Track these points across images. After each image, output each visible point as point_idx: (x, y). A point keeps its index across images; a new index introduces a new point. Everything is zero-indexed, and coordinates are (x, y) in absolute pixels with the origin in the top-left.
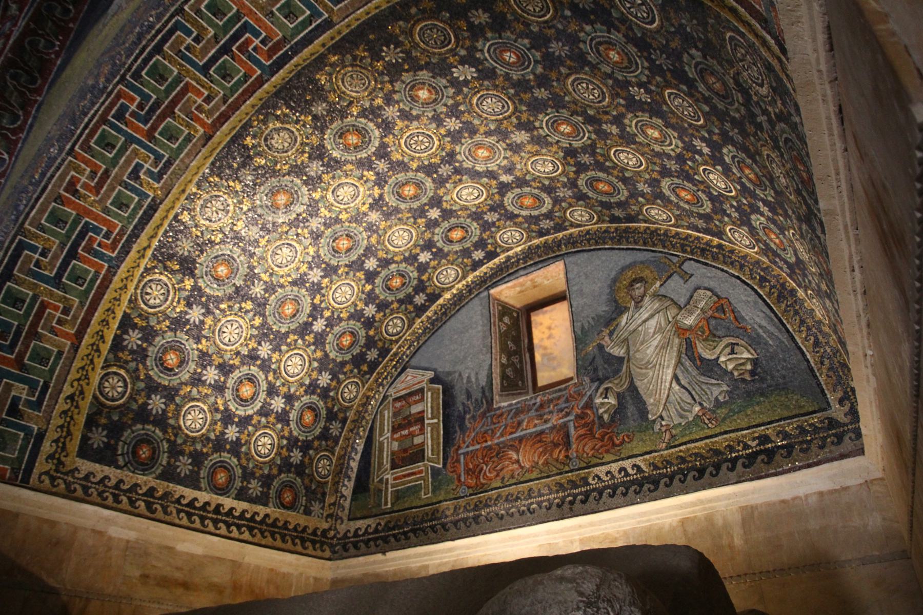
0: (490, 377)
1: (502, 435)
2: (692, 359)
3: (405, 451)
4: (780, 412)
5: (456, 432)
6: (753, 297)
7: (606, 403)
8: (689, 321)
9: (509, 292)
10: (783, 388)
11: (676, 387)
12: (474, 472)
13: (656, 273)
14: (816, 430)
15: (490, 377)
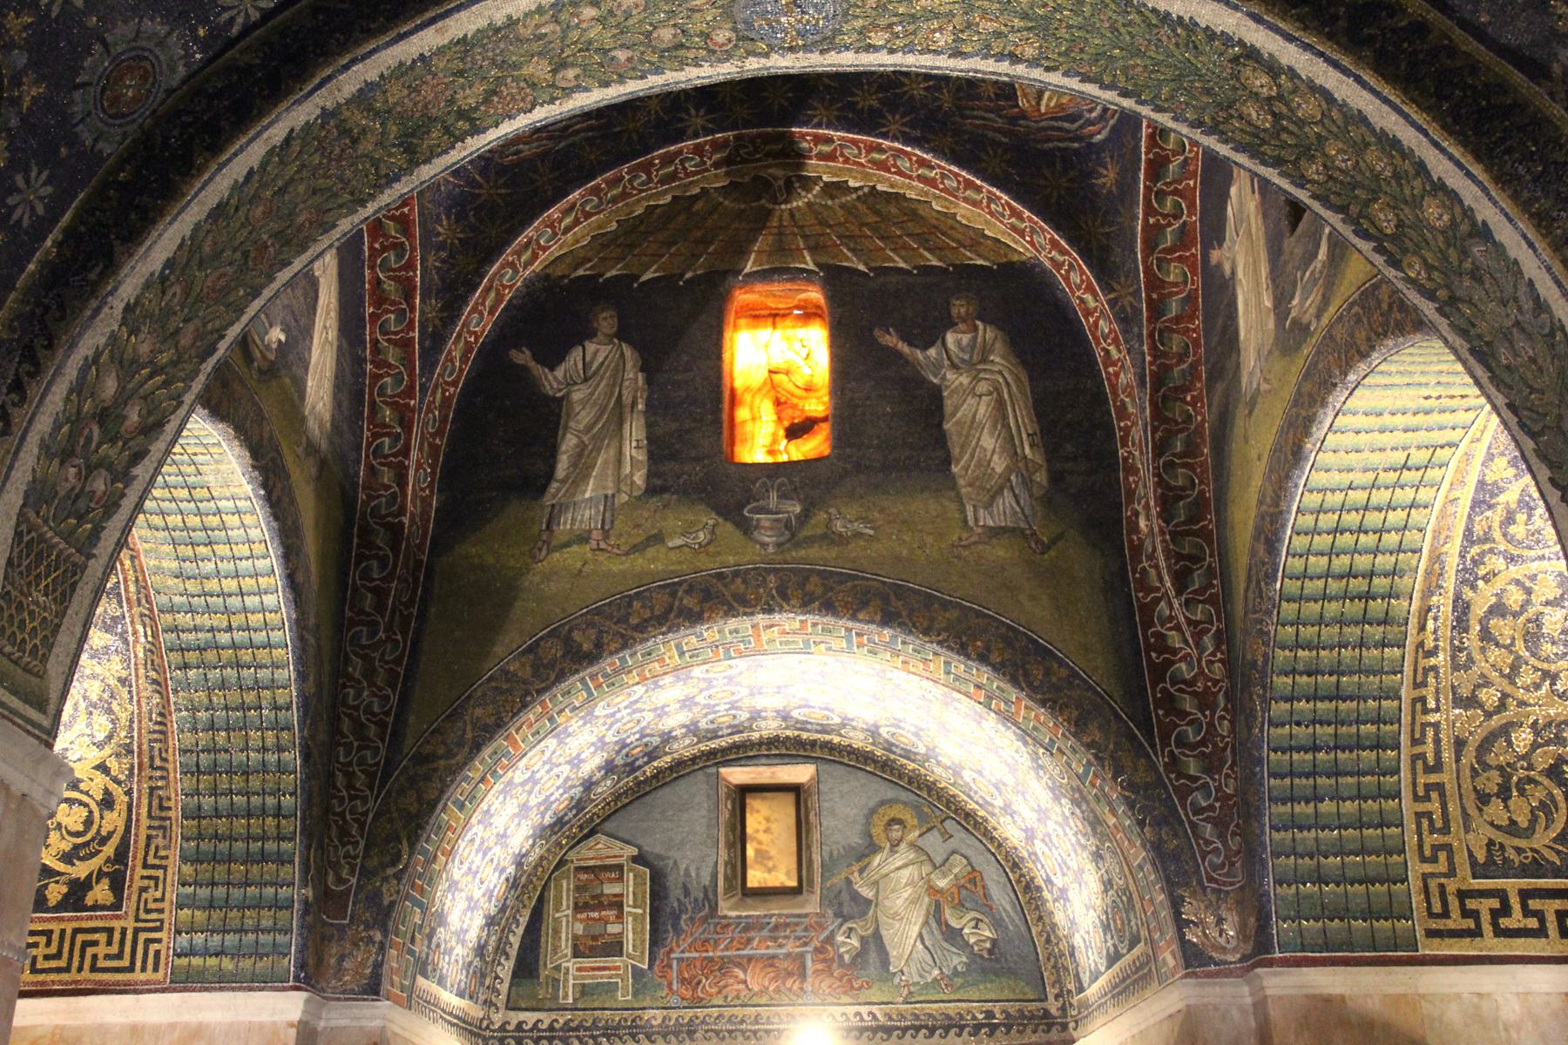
0: (715, 876)
1: (727, 948)
2: (939, 922)
3: (594, 938)
4: (1006, 994)
5: (666, 931)
6: (1004, 879)
7: (848, 944)
8: (942, 883)
9: (738, 775)
10: (1012, 973)
11: (920, 946)
12: (691, 983)
13: (916, 822)
14: (1032, 1017)
15: (715, 876)
